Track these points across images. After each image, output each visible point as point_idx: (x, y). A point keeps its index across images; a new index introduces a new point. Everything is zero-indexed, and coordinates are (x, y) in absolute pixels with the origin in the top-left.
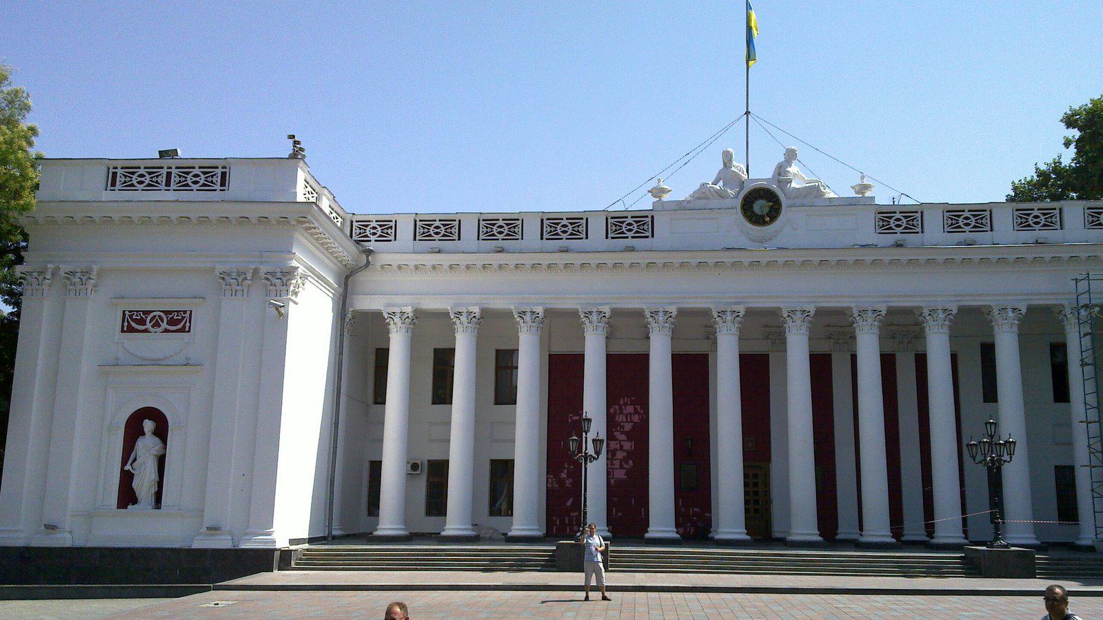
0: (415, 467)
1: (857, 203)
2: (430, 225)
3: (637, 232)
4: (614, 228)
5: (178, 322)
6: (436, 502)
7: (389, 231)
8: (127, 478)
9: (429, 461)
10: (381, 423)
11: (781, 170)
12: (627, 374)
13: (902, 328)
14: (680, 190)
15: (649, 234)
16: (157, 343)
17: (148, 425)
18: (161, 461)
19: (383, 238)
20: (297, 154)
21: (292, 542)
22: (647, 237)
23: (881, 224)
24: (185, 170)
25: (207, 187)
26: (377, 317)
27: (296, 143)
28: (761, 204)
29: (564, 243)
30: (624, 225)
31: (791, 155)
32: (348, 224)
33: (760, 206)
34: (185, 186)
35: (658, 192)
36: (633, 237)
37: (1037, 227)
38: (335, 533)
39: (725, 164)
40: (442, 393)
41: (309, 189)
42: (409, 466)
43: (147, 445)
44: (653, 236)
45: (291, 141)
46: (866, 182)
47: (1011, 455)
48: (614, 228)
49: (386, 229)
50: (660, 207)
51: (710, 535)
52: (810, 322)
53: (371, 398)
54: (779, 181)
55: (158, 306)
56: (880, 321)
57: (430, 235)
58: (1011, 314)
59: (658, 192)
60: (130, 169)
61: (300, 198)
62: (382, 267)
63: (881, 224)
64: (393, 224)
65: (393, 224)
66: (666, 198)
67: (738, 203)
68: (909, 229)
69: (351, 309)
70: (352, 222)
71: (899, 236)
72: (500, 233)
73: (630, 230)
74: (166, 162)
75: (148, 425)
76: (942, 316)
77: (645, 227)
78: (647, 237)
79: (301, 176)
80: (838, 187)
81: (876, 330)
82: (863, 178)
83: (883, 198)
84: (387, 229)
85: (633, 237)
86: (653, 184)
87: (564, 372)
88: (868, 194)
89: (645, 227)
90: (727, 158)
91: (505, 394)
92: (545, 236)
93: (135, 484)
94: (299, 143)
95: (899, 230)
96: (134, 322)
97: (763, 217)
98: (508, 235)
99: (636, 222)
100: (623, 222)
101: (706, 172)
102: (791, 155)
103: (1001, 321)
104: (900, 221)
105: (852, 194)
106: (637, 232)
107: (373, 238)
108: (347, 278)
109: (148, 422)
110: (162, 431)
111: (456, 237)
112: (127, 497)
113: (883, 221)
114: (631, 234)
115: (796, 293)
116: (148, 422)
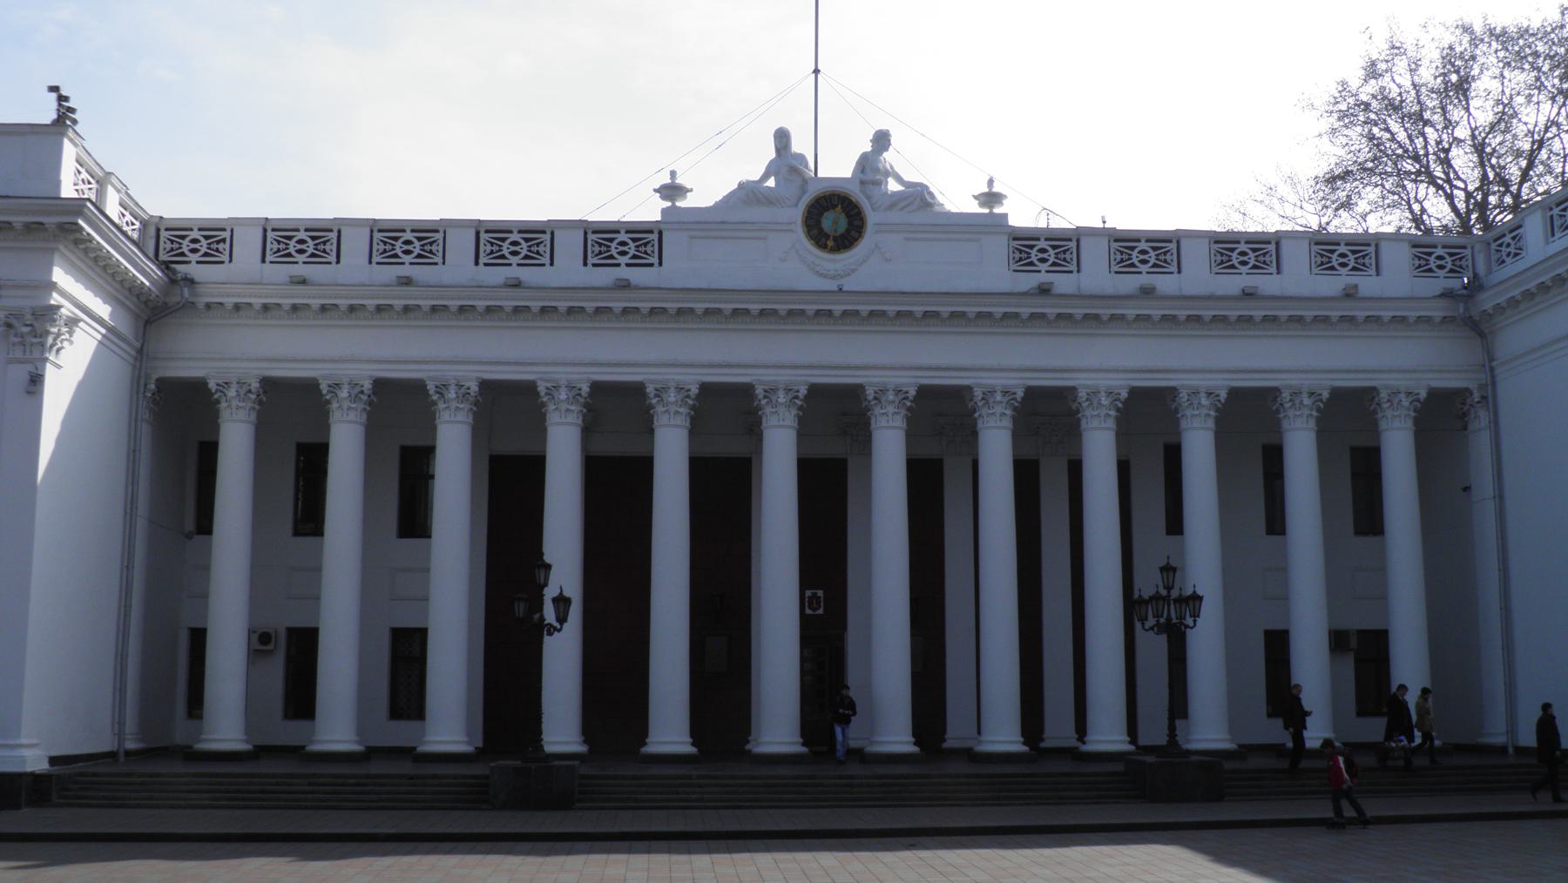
0: (265, 638)
1: (985, 226)
2: (290, 238)
3: (635, 257)
4: (597, 249)
6: (300, 696)
7: (221, 246)
9: (290, 631)
10: (205, 568)
12: (617, 489)
13: (1047, 416)
14: (705, 193)
15: (655, 260)
19: (209, 258)
20: (65, 116)
22: (651, 265)
23: (1017, 255)
27: (62, 99)
28: (836, 216)
29: (514, 272)
30: (614, 245)
31: (882, 140)
32: (152, 231)
33: (833, 222)
36: (628, 265)
37: (1244, 269)
38: (130, 745)
39: (778, 150)
40: (310, 516)
41: (84, 175)
42: (255, 637)
44: (660, 264)
45: (54, 95)
46: (995, 190)
47: (1195, 615)
48: (597, 249)
51: (748, 747)
52: (909, 409)
53: (190, 524)
54: (862, 183)
56: (1015, 409)
57: (289, 255)
58: (1204, 402)
59: (672, 191)
61: (68, 191)
62: (208, 306)
63: (1017, 255)
64: (226, 235)
65: (226, 235)
67: (797, 214)
68: (1058, 266)
69: (155, 377)
70: (158, 230)
71: (1044, 277)
72: (407, 252)
73: (623, 253)
76: (1105, 401)
77: (649, 249)
78: (651, 265)
79: (69, 152)
80: (957, 198)
81: (1007, 423)
82: (991, 182)
83: (1021, 214)
84: (218, 242)
85: (628, 265)
87: (512, 488)
88: (997, 210)
89: (649, 249)
90: (782, 138)
91: (414, 518)
92: (483, 260)
94: (66, 99)
95: (1043, 267)
97: (827, 236)
98: (419, 256)
99: (634, 240)
100: (611, 240)
101: (751, 162)
102: (882, 140)
103: (1189, 412)
105: (974, 208)
106: (635, 257)
107: (194, 257)
108: (147, 323)
111: (333, 258)
114: (623, 260)
115: (889, 363)
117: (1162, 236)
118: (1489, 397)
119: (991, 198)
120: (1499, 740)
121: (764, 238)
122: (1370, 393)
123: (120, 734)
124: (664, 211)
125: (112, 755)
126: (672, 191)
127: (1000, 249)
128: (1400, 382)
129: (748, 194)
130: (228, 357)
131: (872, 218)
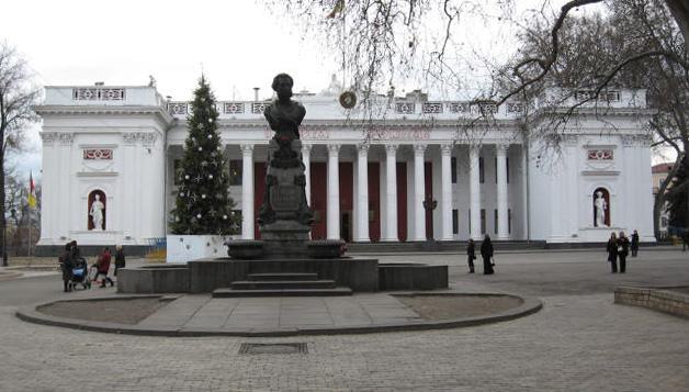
5: (106, 154)
8: (91, 218)
16: (98, 165)
17: (97, 197)
18: (104, 211)
24: (107, 90)
25: (116, 98)
34: (106, 97)
43: (97, 205)
55: (98, 150)
60: (83, 90)
67: (338, 98)
74: (99, 86)
75: (97, 197)
93: (94, 219)
96: (89, 155)
109: (97, 196)
110: (103, 199)
112: (91, 225)
116: (97, 196)
118: (527, 147)
120: (525, 238)
122: (494, 146)
129: (327, 94)
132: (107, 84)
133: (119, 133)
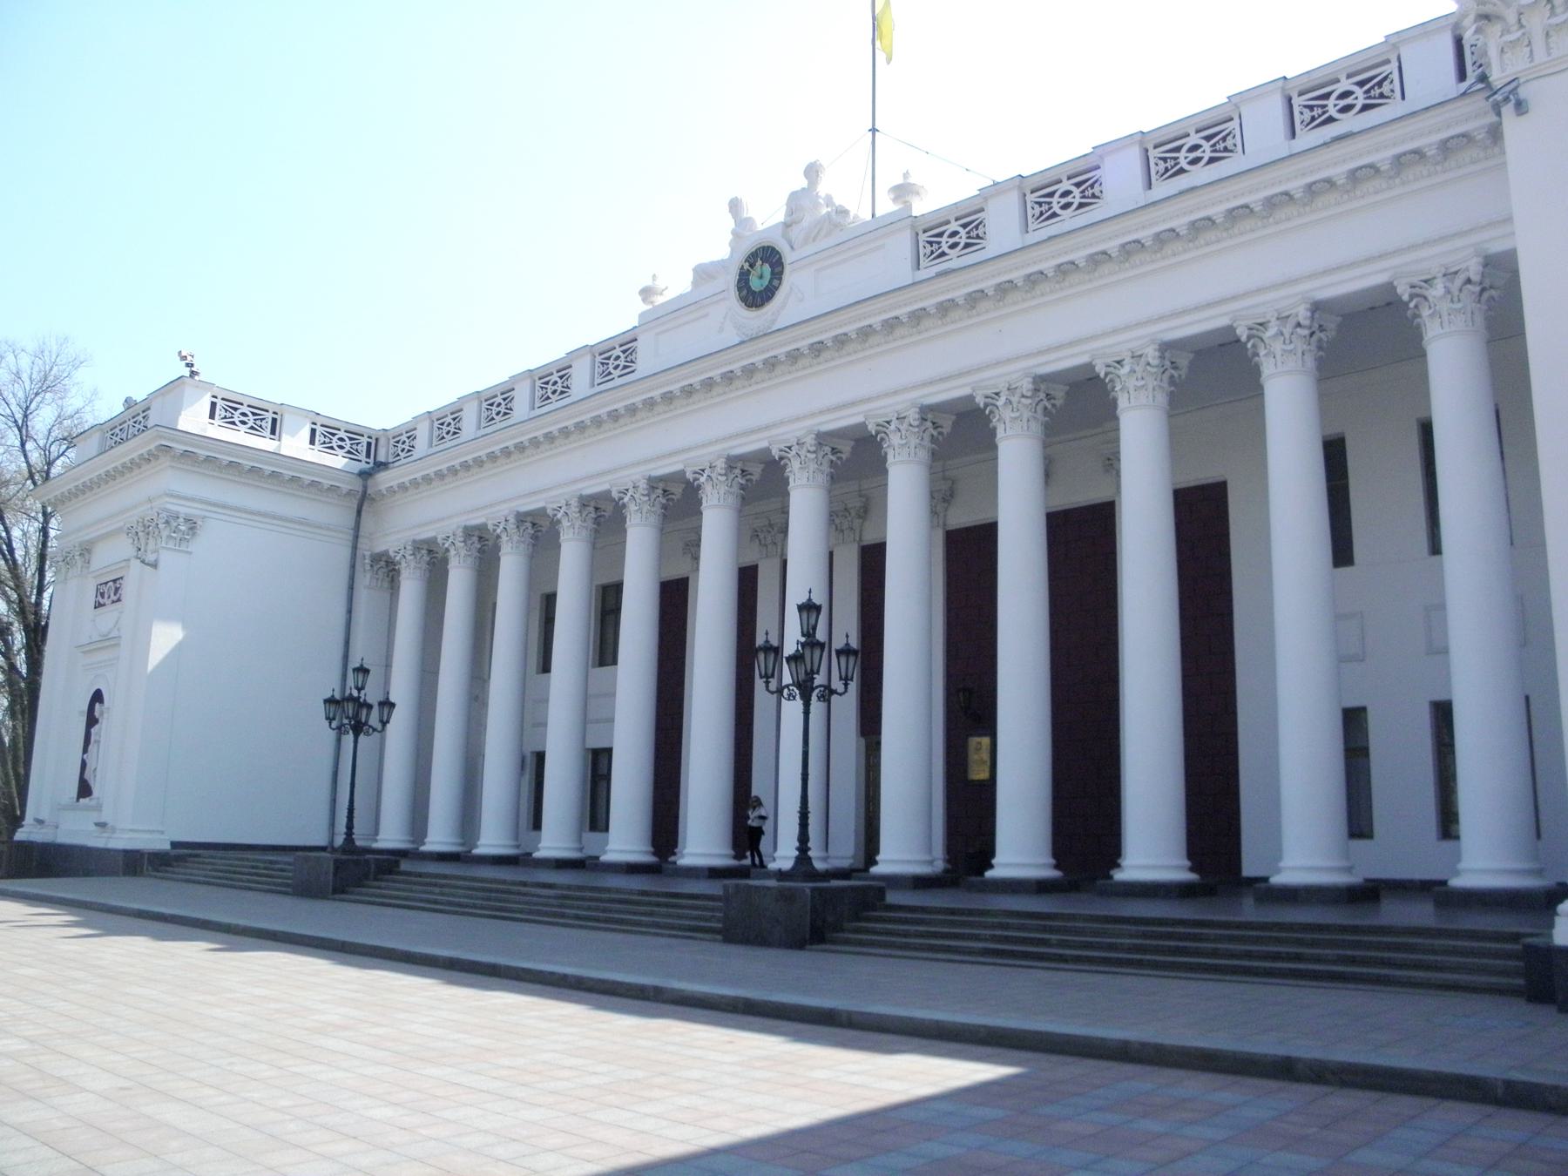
11: (796, 202)
14: (677, 284)
21: (174, 845)
26: (386, 553)
31: (812, 172)
35: (646, 293)
46: (911, 180)
49: (404, 439)
50: (651, 321)
66: (659, 300)
67: (732, 278)
82: (906, 175)
86: (649, 283)
90: (735, 206)
102: (812, 172)
104: (951, 235)
108: (359, 512)
112: (85, 790)
113: (931, 243)
114: (618, 372)
117: (1082, 166)
119: (903, 191)
121: (706, 316)
123: (332, 834)
124: (642, 315)
125: (323, 849)
126: (646, 293)
127: (902, 246)
128: (1432, 260)
129: (703, 274)
130: (403, 525)
131: (788, 257)
132: (139, 396)
133: (119, 530)
